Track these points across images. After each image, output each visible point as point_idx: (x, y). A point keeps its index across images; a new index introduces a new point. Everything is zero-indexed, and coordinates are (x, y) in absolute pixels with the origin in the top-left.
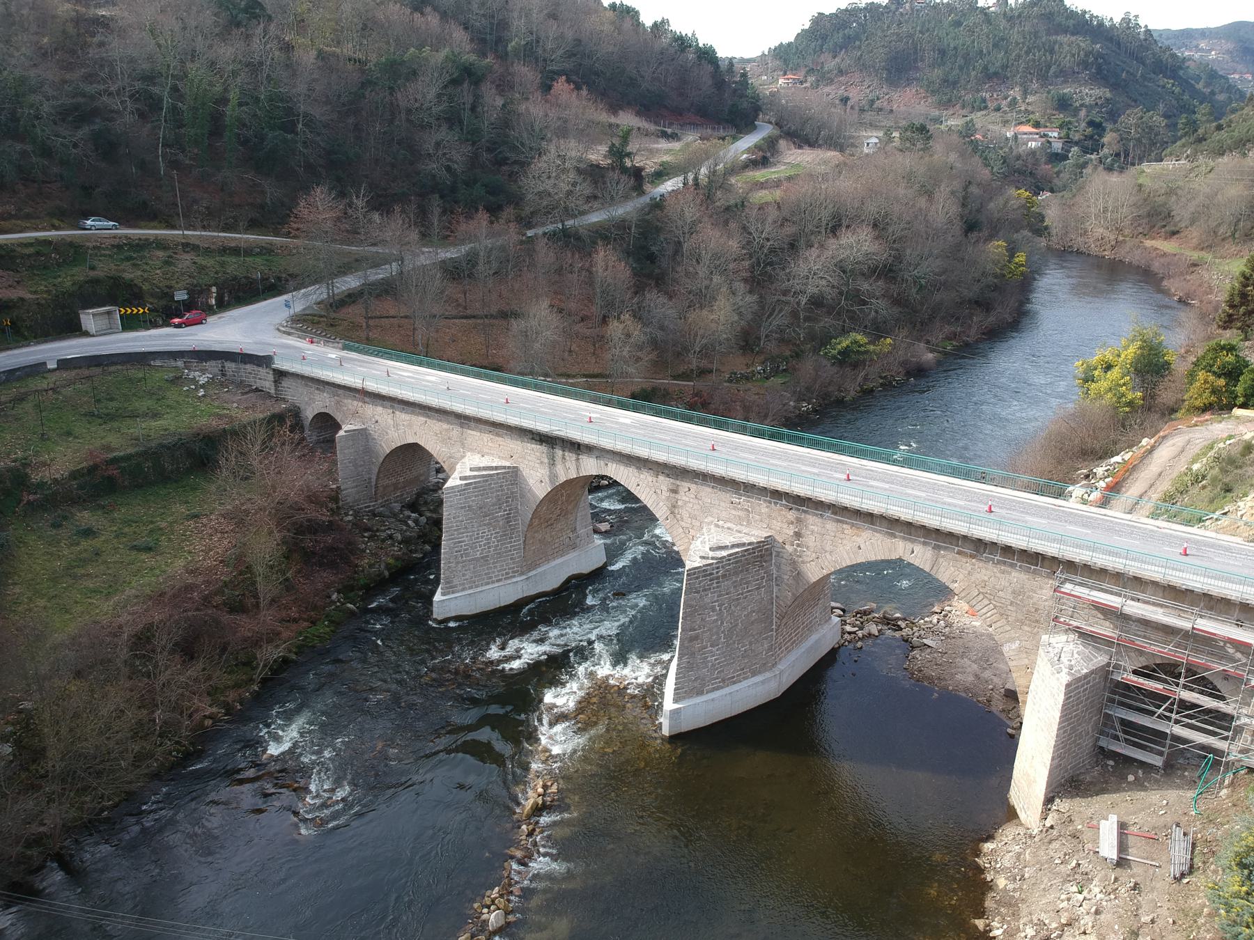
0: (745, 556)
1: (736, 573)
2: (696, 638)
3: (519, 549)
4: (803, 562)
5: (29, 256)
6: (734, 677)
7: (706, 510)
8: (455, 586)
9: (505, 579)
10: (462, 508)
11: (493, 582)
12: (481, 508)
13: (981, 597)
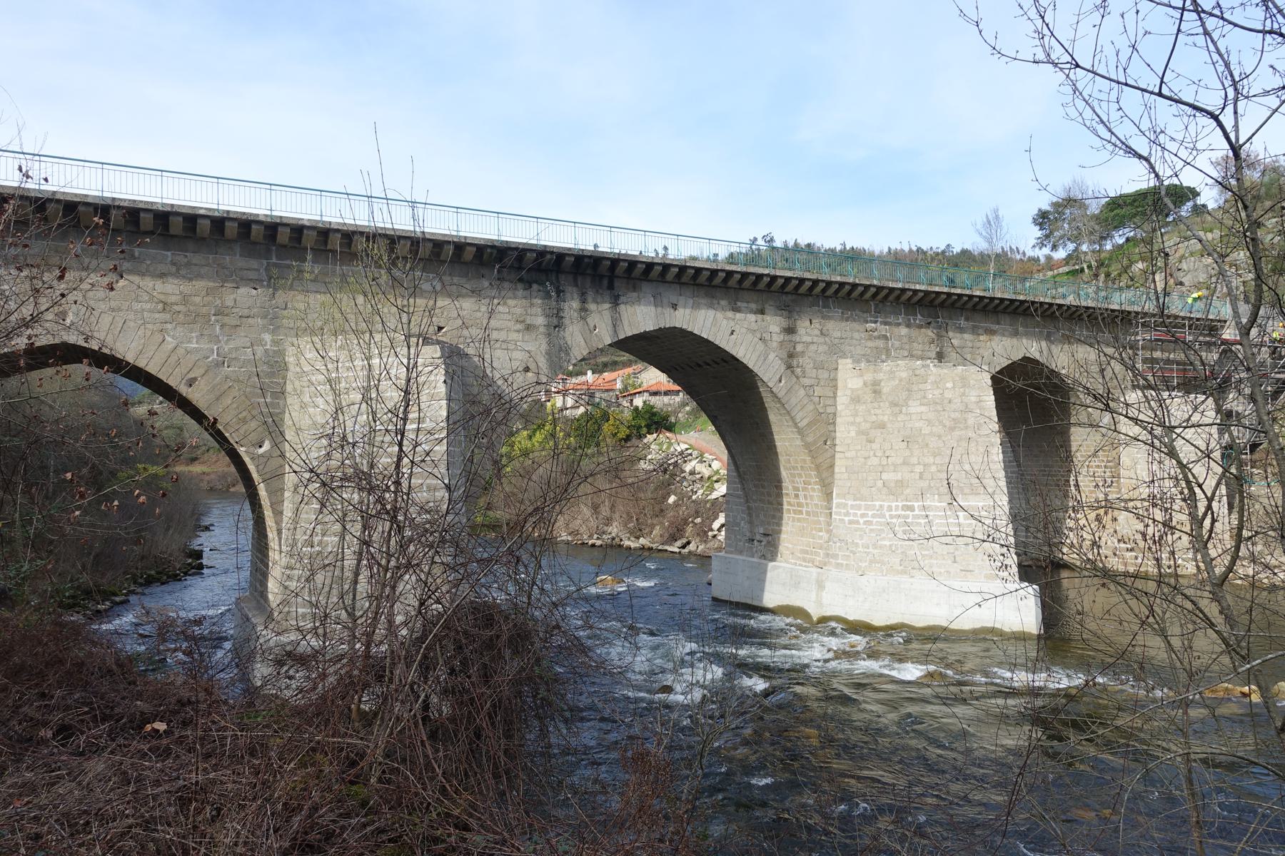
7: (836, 351)
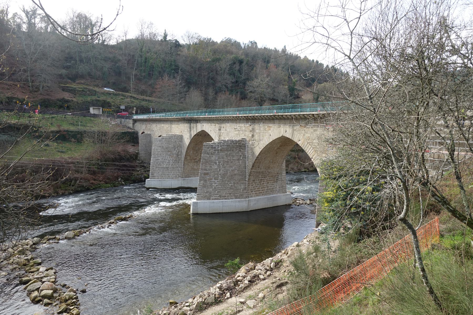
0: (232, 144)
1: (227, 150)
2: (207, 174)
4: (255, 147)
5: (80, 91)
6: (226, 196)
8: (155, 176)
9: (175, 178)
10: (160, 147)
11: (170, 178)
12: (167, 148)
13: (308, 144)
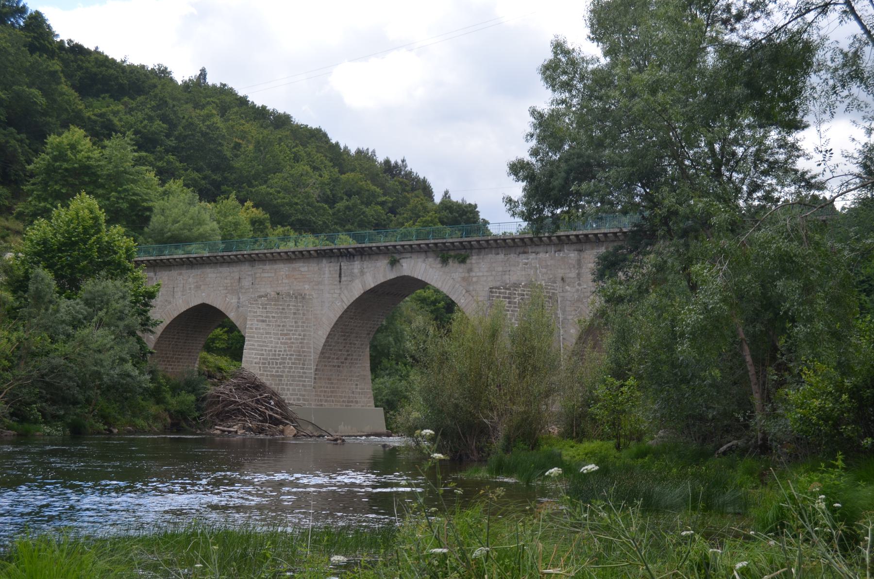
3: (311, 377)
